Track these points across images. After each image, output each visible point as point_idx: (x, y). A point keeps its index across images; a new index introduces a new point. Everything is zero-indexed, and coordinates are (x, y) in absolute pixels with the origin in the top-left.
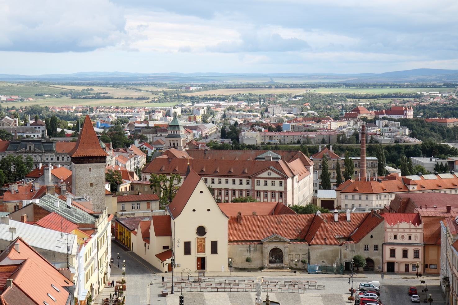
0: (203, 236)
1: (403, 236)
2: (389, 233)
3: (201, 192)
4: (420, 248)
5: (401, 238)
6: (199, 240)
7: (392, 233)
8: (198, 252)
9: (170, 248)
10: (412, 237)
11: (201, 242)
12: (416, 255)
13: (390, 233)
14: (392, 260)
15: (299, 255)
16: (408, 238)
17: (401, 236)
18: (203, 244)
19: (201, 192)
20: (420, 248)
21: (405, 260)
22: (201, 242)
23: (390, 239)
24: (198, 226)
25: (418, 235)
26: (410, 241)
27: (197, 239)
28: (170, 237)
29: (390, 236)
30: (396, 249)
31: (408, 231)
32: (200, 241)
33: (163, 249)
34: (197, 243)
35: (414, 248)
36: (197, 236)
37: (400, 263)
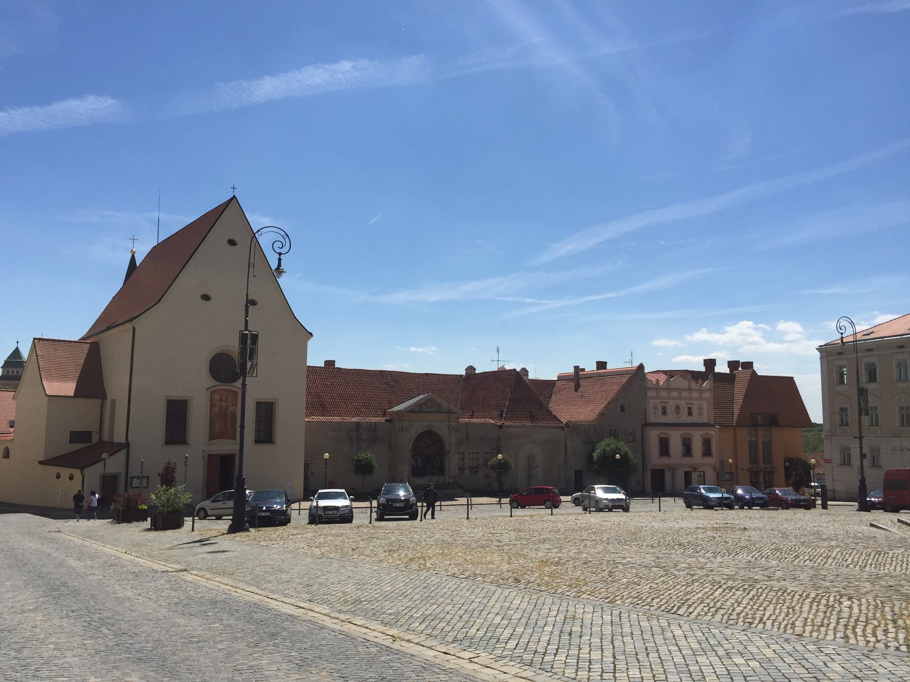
0: (232, 384)
1: (678, 408)
2: (652, 401)
3: (232, 243)
4: (712, 433)
5: (674, 413)
6: (217, 397)
7: (658, 401)
8: (213, 436)
9: (95, 439)
10: (695, 411)
11: (224, 404)
12: (707, 452)
13: (654, 401)
14: (665, 461)
15: (477, 453)
16: (686, 411)
17: (674, 408)
18: (230, 409)
19: (232, 243)
20: (712, 433)
21: (687, 460)
22: (224, 404)
23: (655, 414)
24: (213, 354)
25: (704, 404)
26: (690, 420)
27: (212, 392)
28: (98, 402)
29: (656, 408)
30: (670, 435)
31: (685, 394)
32: (221, 401)
33: (70, 442)
34: (212, 405)
35: (702, 433)
36: (211, 382)
37: (673, 469)
